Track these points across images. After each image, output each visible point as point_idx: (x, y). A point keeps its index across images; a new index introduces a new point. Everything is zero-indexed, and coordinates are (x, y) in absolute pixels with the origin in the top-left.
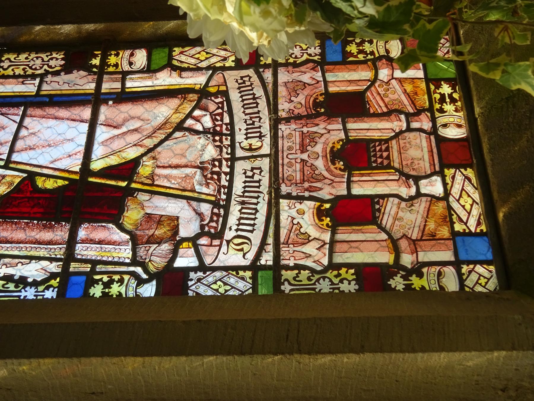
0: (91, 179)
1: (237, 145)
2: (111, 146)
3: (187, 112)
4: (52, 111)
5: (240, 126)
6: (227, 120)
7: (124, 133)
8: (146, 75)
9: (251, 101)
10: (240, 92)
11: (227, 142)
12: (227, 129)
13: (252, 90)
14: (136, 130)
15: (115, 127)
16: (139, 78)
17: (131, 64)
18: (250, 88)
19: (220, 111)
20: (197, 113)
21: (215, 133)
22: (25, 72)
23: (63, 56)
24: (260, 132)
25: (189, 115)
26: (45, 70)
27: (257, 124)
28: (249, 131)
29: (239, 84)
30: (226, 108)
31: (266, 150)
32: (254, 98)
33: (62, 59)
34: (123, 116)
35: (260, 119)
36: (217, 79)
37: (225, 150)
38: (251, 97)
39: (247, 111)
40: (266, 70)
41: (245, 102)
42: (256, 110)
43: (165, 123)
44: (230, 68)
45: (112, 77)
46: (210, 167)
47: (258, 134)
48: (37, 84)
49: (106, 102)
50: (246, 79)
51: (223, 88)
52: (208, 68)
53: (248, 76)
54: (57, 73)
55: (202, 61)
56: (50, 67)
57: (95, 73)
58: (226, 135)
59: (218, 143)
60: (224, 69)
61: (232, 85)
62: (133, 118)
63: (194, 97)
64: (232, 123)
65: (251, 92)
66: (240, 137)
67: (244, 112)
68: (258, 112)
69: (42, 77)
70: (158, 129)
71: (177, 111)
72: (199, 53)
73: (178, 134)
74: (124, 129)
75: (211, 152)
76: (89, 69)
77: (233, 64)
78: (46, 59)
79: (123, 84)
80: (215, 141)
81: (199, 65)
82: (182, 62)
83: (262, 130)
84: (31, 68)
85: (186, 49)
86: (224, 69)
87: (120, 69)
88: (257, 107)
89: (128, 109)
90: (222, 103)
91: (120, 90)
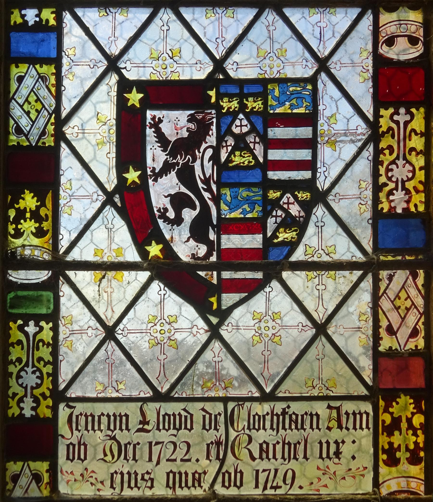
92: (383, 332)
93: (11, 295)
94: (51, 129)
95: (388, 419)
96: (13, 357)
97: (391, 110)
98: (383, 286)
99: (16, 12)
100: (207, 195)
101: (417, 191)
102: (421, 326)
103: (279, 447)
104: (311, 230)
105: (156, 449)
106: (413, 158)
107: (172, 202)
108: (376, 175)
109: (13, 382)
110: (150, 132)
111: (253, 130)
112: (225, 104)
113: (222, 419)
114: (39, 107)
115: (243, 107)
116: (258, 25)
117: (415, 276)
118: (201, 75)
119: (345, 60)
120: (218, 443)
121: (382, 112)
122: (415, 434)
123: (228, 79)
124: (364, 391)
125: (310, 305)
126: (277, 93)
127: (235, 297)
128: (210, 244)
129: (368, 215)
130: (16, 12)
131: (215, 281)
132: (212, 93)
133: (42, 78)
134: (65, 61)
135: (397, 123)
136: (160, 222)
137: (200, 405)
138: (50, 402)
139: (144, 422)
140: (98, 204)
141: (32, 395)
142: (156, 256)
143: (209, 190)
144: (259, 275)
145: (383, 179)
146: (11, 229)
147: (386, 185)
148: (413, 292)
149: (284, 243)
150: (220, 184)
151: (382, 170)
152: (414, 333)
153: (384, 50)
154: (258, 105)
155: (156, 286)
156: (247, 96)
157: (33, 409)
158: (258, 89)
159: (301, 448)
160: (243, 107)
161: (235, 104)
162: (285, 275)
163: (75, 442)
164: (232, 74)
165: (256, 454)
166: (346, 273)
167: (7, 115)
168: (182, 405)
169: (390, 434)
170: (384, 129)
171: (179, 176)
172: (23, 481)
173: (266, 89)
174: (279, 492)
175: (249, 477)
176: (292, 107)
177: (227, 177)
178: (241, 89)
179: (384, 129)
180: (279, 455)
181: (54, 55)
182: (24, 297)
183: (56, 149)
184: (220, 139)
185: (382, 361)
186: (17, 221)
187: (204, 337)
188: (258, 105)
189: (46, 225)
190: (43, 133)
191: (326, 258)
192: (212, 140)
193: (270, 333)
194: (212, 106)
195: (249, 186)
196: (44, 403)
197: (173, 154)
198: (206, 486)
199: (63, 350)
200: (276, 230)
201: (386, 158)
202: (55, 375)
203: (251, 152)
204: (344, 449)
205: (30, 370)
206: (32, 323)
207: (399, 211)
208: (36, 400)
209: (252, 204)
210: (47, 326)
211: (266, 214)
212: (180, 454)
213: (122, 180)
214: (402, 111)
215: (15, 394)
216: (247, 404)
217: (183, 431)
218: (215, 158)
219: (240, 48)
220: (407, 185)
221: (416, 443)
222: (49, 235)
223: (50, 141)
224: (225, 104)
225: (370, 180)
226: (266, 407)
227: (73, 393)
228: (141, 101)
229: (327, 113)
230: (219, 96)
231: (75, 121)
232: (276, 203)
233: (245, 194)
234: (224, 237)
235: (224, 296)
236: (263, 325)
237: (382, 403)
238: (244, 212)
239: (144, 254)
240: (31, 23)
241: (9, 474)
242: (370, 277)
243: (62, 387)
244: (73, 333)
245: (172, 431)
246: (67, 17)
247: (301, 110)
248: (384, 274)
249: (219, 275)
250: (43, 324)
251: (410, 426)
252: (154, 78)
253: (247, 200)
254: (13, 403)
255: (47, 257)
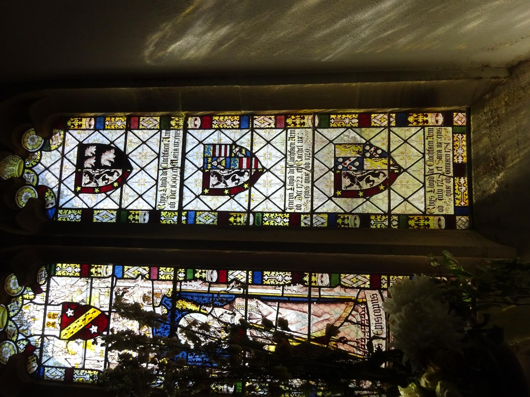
0: (312, 343)
1: (372, 331)
2: (318, 326)
3: (349, 312)
4: (290, 305)
5: (373, 321)
6: (367, 318)
7: (323, 321)
8: (329, 289)
9: (377, 309)
10: (372, 303)
11: (367, 330)
12: (367, 323)
13: (377, 302)
14: (327, 319)
15: (318, 317)
16: (327, 290)
17: (322, 282)
18: (377, 301)
19: (363, 312)
20: (354, 313)
21: (363, 325)
22: (275, 283)
23: (290, 275)
24: (381, 326)
25: (350, 314)
26: (284, 282)
27: (380, 321)
28: (377, 325)
29: (372, 298)
30: (366, 312)
31: (384, 336)
32: (379, 307)
33: (291, 276)
34: (321, 311)
35: (382, 319)
36: (362, 294)
37: (366, 333)
38: (377, 306)
39: (376, 314)
40: (384, 291)
41: (375, 309)
42: (379, 314)
43: (340, 317)
44: (367, 289)
45: (314, 289)
46: (360, 342)
47: (380, 327)
48: (281, 290)
49: (313, 302)
50: (375, 296)
51: (364, 300)
52: (357, 288)
53: (376, 294)
54: (289, 285)
55: (354, 283)
56: (286, 280)
57: (306, 286)
58: (367, 326)
59: (363, 330)
60: (365, 289)
61: (369, 299)
62: (326, 313)
63: (351, 303)
64: (369, 320)
65: (377, 304)
66: (373, 328)
67: (374, 314)
68: (380, 315)
69: (283, 286)
70: (337, 320)
71: (345, 311)
72: (353, 278)
73: (346, 324)
74: (322, 319)
75: (361, 335)
76: (303, 282)
77: (369, 286)
78: (284, 276)
79: (320, 293)
80: (362, 329)
81: (353, 285)
82: (345, 283)
83: (382, 325)
84: (277, 280)
85: (347, 275)
86: (365, 289)
87: (317, 285)
88: (380, 312)
89: (323, 308)
90: (364, 308)
91: (318, 297)
92: (270, 127)
93: (256, 224)
94: (213, 213)
95: (293, 125)
96: (273, 224)
97: (213, 125)
98: (258, 127)
99: (183, 222)
100: (232, 172)
101: (234, 118)
102: (268, 117)
103: (299, 153)
104: (243, 145)
105: (299, 186)
106: (225, 120)
107: (234, 181)
108: (229, 129)
109: (279, 224)
110: (215, 187)
111: (216, 160)
112: (209, 167)
113: (291, 168)
114: (207, 216)
115: (210, 163)
116: (189, 159)
117: (255, 118)
118: (202, 173)
119: (200, 136)
120: (298, 169)
121: (213, 127)
122: (297, 118)
123: (203, 167)
124: (285, 132)
125: (263, 145)
126: (207, 154)
127: (259, 165)
128: (245, 171)
129: (239, 131)
130: (183, 222)
131: (255, 170)
132: (206, 171)
133: (200, 215)
134: (196, 209)
135: (216, 123)
136: (239, 184)
137: (287, 174)
138: (285, 214)
139: (291, 189)
140: (233, 201)
141: (283, 219)
142: (248, 186)
143: (231, 172)
144: (254, 159)
145: (230, 127)
146: (239, 224)
147: (232, 126)
148: (260, 119)
149: (246, 152)
150: (230, 169)
151: (228, 127)
152: (270, 118)
153: (198, 127)
154: (210, 159)
155: (255, 186)
156: (207, 162)
157: (287, 219)
158: (206, 159)
159: (300, 148)
160: (210, 163)
161: (209, 165)
162: (254, 152)
163: (296, 208)
164: (202, 166)
165: (301, 159)
166: (254, 136)
167: (209, 225)
168: (287, 179)
169: (297, 124)
170: (218, 127)
171: (227, 179)
172: (306, 222)
173: (206, 157)
174: (311, 153)
175: (307, 161)
176: (211, 150)
177: (228, 167)
178: (206, 163)
179: (218, 127)
180: (301, 153)
181: (194, 212)
182: (257, 221)
183: (218, 212)
184: (218, 169)
185: (278, 126)
186: (237, 223)
187: (269, 173)
188: (210, 159)
189: (238, 215)
190: (214, 215)
191: (250, 141)
192: (218, 171)
193: (269, 156)
194: (210, 171)
195: (230, 161)
196: (285, 216)
197: (221, 181)
198: (309, 173)
199: (271, 211)
200: (242, 154)
201: (225, 126)
202: (278, 213)
203: (222, 161)
204: (300, 137)
205: (276, 220)
206: (264, 219)
207: (239, 123)
208: (284, 218)
209: (235, 160)
210: (265, 215)
211: (238, 157)
212: (300, 180)
213: (228, 194)
214: (213, 122)
215: (283, 224)
216: (287, 162)
217: (294, 179)
218: (223, 170)
219: (195, 164)
220: (232, 121)
221: (299, 118)
222: (241, 214)
223: (216, 214)
224: (209, 167)
225: (231, 130)
226: (289, 157)
227: (283, 208)
228: (207, 189)
229: (213, 141)
230: (207, 169)
231: (211, 207)
232: (235, 154)
233: (232, 162)
234: (244, 168)
235: (259, 168)
236: (267, 158)
237: (288, 127)
238: (237, 162)
239: (247, 189)
240: (186, 218)
241: (304, 226)
242: (255, 130)
243: (281, 211)
244: (267, 208)
245: (294, 181)
246: (185, 209)
247: (212, 148)
248: (255, 126)
249: (253, 169)
250: (264, 216)
251: (294, 119)
252: (202, 186)
253: (234, 162)
254: (285, 224)
255: (246, 215)
